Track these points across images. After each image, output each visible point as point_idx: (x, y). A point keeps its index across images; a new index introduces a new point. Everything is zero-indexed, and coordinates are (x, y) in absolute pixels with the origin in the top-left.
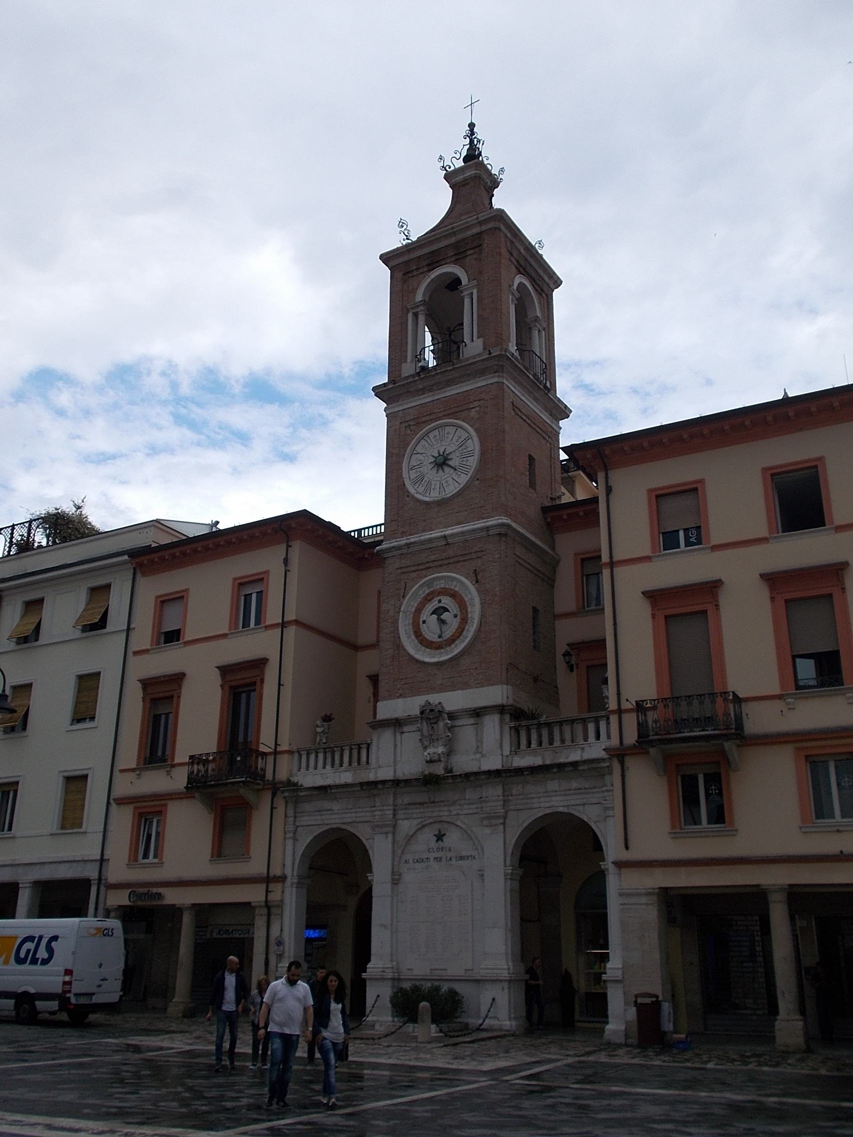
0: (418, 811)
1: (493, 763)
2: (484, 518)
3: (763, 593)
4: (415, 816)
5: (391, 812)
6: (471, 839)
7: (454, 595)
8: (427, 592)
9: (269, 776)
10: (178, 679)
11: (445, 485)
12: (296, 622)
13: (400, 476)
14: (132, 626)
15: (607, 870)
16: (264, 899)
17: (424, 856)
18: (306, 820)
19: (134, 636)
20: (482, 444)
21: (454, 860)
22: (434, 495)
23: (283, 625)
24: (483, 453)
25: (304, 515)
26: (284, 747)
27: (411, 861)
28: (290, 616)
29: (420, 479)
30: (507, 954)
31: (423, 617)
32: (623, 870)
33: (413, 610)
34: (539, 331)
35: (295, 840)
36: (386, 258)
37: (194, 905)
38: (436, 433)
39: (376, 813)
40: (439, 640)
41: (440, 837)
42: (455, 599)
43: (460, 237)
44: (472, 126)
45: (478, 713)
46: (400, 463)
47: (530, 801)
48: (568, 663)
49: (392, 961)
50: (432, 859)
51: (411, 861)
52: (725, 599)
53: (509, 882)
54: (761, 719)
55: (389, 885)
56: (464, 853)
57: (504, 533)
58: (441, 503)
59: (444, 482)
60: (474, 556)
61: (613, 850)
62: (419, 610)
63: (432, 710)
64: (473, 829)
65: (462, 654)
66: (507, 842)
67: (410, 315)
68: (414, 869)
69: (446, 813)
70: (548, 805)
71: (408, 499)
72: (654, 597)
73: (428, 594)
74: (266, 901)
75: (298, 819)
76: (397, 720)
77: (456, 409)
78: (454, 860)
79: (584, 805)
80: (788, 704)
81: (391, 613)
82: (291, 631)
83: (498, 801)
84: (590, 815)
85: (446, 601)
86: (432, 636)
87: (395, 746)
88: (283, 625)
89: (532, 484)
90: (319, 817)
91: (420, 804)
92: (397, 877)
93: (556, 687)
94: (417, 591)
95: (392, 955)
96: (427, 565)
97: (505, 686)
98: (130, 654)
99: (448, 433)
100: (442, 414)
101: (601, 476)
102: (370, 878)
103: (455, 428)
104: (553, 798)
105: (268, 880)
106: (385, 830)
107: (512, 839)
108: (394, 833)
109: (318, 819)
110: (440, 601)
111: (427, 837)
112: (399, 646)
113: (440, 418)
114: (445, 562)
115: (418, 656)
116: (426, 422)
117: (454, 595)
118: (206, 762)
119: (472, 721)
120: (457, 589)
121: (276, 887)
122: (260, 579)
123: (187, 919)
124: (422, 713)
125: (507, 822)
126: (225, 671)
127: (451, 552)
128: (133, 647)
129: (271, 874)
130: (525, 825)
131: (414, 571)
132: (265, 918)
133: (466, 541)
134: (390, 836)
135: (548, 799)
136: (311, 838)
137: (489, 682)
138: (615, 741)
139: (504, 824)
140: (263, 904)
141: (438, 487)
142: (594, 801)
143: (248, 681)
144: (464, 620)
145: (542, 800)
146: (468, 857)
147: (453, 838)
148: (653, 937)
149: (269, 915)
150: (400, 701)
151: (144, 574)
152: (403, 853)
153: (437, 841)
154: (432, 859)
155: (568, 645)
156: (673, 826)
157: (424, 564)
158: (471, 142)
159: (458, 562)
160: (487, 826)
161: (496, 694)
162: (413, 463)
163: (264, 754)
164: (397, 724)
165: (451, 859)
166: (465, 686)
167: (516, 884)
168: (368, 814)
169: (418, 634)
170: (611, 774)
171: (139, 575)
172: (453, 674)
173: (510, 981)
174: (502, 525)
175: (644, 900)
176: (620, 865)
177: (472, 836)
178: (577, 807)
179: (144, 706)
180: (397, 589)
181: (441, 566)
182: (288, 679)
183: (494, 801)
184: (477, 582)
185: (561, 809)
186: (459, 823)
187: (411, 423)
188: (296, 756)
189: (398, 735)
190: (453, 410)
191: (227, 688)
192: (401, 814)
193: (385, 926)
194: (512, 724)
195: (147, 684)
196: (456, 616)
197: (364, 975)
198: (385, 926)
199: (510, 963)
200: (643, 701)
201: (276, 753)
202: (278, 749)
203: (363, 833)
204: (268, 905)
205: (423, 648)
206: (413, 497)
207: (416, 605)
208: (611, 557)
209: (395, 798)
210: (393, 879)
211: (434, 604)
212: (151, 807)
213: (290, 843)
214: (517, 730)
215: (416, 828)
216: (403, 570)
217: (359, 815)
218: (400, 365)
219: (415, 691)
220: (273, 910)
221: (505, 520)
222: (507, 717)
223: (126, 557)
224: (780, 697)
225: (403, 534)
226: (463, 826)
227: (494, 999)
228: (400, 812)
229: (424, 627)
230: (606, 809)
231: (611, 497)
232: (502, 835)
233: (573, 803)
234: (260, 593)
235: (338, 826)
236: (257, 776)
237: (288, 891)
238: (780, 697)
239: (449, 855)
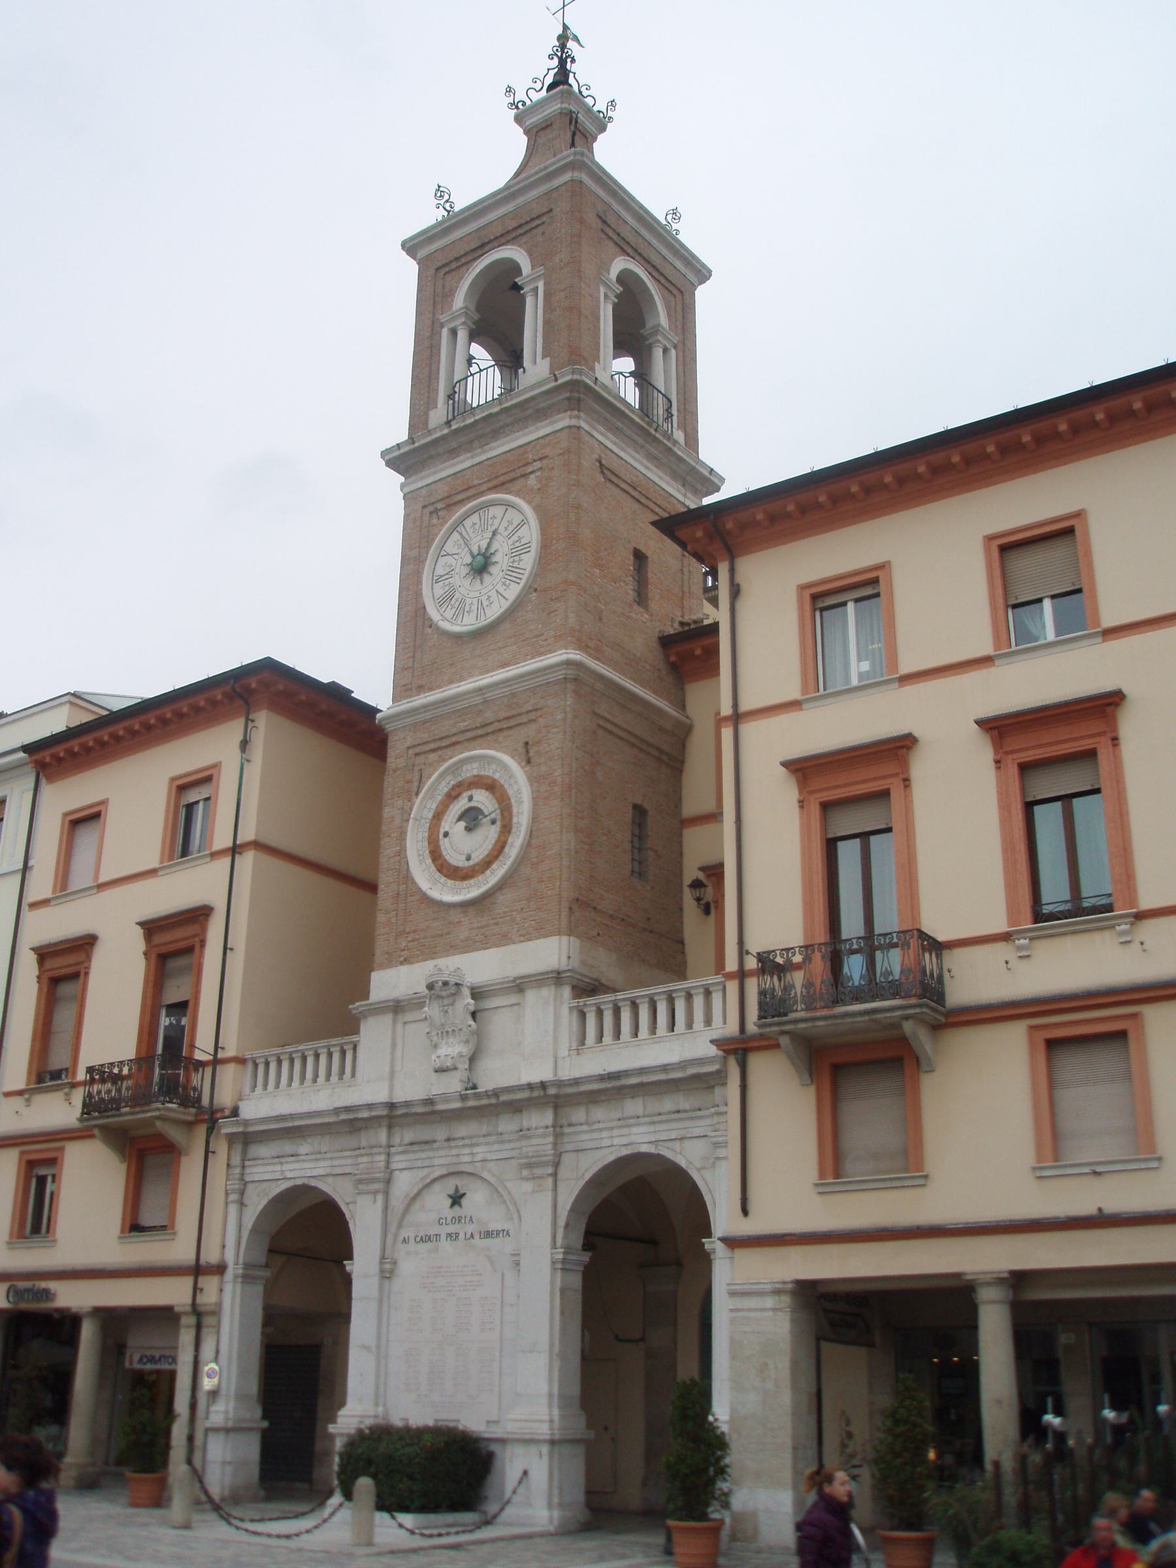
0: (424, 1155)
1: (538, 1072)
2: (542, 654)
3: (982, 753)
4: (419, 1163)
5: (383, 1157)
6: (504, 1202)
7: (492, 786)
8: (453, 783)
9: (205, 1101)
10: (85, 944)
11: (485, 603)
12: (257, 845)
13: (418, 594)
14: (31, 863)
15: (714, 1251)
16: (189, 1300)
17: (432, 1232)
18: (257, 1172)
19: (33, 878)
20: (544, 531)
21: (477, 1236)
22: (468, 623)
23: (235, 850)
24: (545, 546)
25: (268, 667)
26: (230, 1051)
27: (412, 1241)
28: (248, 833)
29: (448, 597)
30: (550, 1396)
31: (445, 826)
32: (739, 1252)
33: (430, 815)
34: (665, 350)
35: (242, 1204)
36: (411, 247)
38: (475, 518)
39: (360, 1160)
40: (467, 864)
41: (456, 1199)
42: (493, 794)
43: (520, 200)
44: (563, 39)
45: (519, 986)
46: (418, 573)
47: (595, 1135)
48: (698, 900)
49: (377, 1405)
50: (443, 1237)
51: (412, 1241)
52: (921, 768)
53: (559, 1273)
54: (975, 979)
55: (376, 1280)
56: (494, 1226)
57: (576, 677)
58: (478, 634)
59: (484, 598)
60: (524, 719)
61: (724, 1218)
62: (438, 816)
63: (445, 984)
64: (508, 1184)
65: (500, 886)
66: (559, 1206)
67: (445, 332)
68: (417, 1253)
69: (467, 1159)
70: (625, 1141)
71: (429, 631)
73: (453, 788)
74: (194, 1304)
75: (247, 1171)
76: (397, 1001)
77: (506, 477)
78: (477, 1236)
79: (681, 1139)
80: (1019, 948)
81: (397, 822)
82: (247, 861)
83: (544, 1136)
84: (688, 1156)
85: (482, 799)
86: (455, 858)
87: (394, 1045)
88: (235, 850)
89: (641, 598)
90: (278, 1168)
91: (426, 1143)
92: (388, 1266)
93: (682, 943)
94: (437, 783)
95: (377, 1396)
96: (454, 739)
97: (565, 939)
98: (25, 907)
99: (494, 517)
100: (485, 487)
101: (723, 569)
102: (348, 1268)
104: (635, 1130)
105: (197, 1270)
106: (376, 1186)
107: (567, 1200)
108: (387, 1193)
109: (278, 1172)
110: (470, 799)
111: (438, 1199)
112: (408, 878)
113: (482, 494)
114: (479, 732)
115: (435, 894)
116: (461, 502)
117: (492, 786)
118: (117, 1079)
119: (513, 999)
120: (497, 776)
121: (210, 1284)
122: (205, 778)
123: (87, 1332)
124: (430, 987)
125: (562, 1173)
126: (151, 928)
127: (489, 715)
128: (32, 896)
129: (202, 1261)
130: (588, 1176)
131: (433, 751)
132: (193, 1332)
133: (514, 695)
134: (380, 1197)
135: (625, 1131)
136: (264, 1202)
137: (540, 931)
138: (732, 1028)
139: (555, 1175)
140: (189, 1309)
141: (474, 608)
142: (697, 1132)
143: (183, 944)
144: (506, 829)
145: (616, 1132)
146: (498, 1233)
147: (476, 1199)
148: (781, 1366)
149: (199, 1327)
150: (404, 969)
151: (51, 779)
152: (400, 1226)
153: (452, 1205)
154: (443, 1237)
155: (702, 869)
156: (822, 1174)
157: (448, 737)
158: (562, 63)
159: (501, 730)
160: (527, 1179)
161: (551, 952)
162: (440, 571)
163: (202, 1064)
164: (397, 1008)
165: (472, 1236)
166: (504, 940)
167: (576, 1280)
168: (349, 1161)
169: (436, 855)
170: (724, 1084)
171: (43, 781)
172: (483, 920)
173: (552, 1442)
174: (568, 663)
175: (769, 1302)
176: (733, 1243)
177: (505, 1194)
178: (669, 1144)
179: (40, 990)
180: (410, 782)
181: (474, 738)
182: (239, 938)
183: (540, 1136)
184: (529, 762)
185: (644, 1149)
186: (486, 1175)
187: (440, 505)
188: (250, 1066)
189: (399, 1025)
190: (501, 479)
191: (154, 956)
192: (398, 1161)
193: (367, 1348)
194: (574, 1003)
195: (44, 954)
196: (493, 822)
197: (331, 1428)
198: (367, 1348)
199: (556, 1412)
200: (769, 952)
201: (216, 1062)
202: (219, 1056)
203: (340, 1192)
204: (197, 1312)
205: (443, 878)
207: (434, 806)
208: (735, 705)
209: (389, 1135)
210: (382, 1271)
211: (461, 804)
212: (41, 1151)
213: (233, 1209)
214: (583, 1015)
215: (421, 1186)
216: (417, 750)
217: (336, 1162)
218: (427, 414)
219: (429, 952)
220: (208, 1321)
221: (574, 655)
222: (567, 991)
223: (22, 755)
224: (1006, 937)
225: (421, 689)
226: (492, 1181)
227: (525, 1473)
228: (396, 1158)
229: (444, 843)
230: (716, 1145)
231: (740, 605)
232: (549, 1195)
233: (663, 1136)
234: (208, 799)
235: (306, 1181)
236: (189, 1100)
237: (228, 1288)
238: (1006, 937)
239: (470, 1228)
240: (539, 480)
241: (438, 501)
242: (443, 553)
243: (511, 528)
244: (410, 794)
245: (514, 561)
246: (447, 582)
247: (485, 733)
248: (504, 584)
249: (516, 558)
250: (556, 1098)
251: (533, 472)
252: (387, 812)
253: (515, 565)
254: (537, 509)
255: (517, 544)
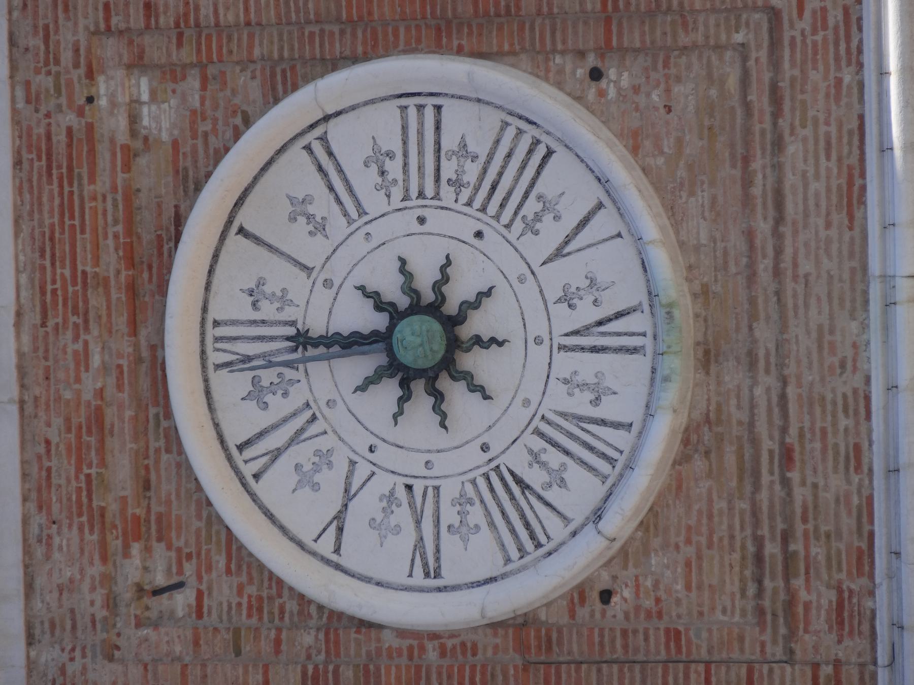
11: (587, 314)
59: (567, 319)
71: (624, 596)
99: (255, 294)
103: (234, 241)
141: (588, 366)
190: (111, 260)
206: (623, 555)
240: (173, 74)
241: (107, 580)
242: (326, 546)
243: (323, 206)
245: (457, 184)
246: (449, 516)
248: (531, 228)
249: (448, 171)
251: (134, 119)
253: (472, 171)
254: (281, 83)
255: (394, 168)
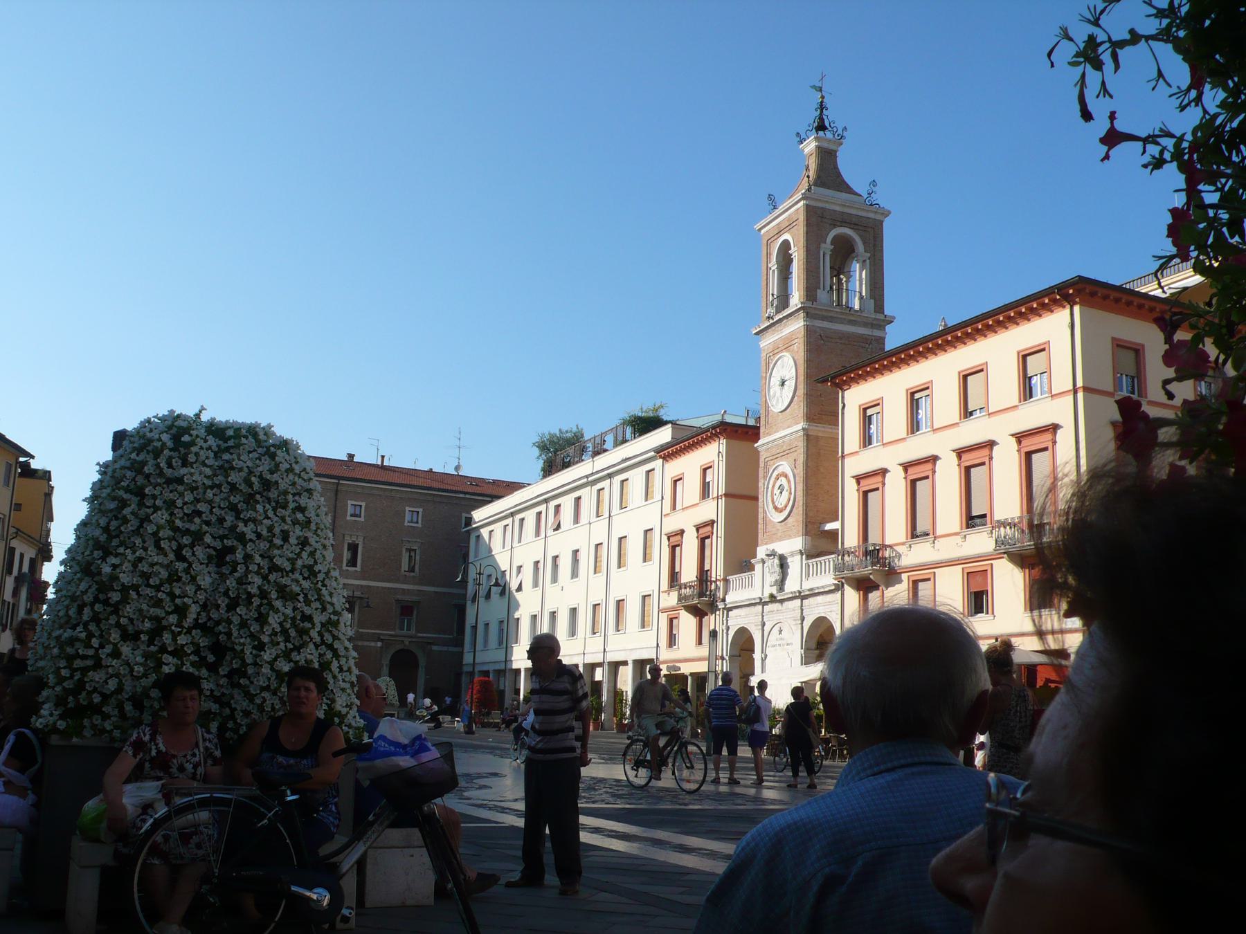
37: (691, 674)
41: (780, 632)
45: (792, 555)
72: (859, 479)
85: (783, 481)
164: (763, 562)
244: (765, 477)
247: (784, 454)
250: (801, 596)
252: (761, 484)
